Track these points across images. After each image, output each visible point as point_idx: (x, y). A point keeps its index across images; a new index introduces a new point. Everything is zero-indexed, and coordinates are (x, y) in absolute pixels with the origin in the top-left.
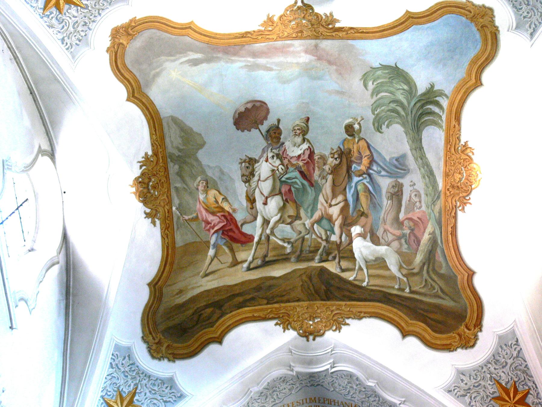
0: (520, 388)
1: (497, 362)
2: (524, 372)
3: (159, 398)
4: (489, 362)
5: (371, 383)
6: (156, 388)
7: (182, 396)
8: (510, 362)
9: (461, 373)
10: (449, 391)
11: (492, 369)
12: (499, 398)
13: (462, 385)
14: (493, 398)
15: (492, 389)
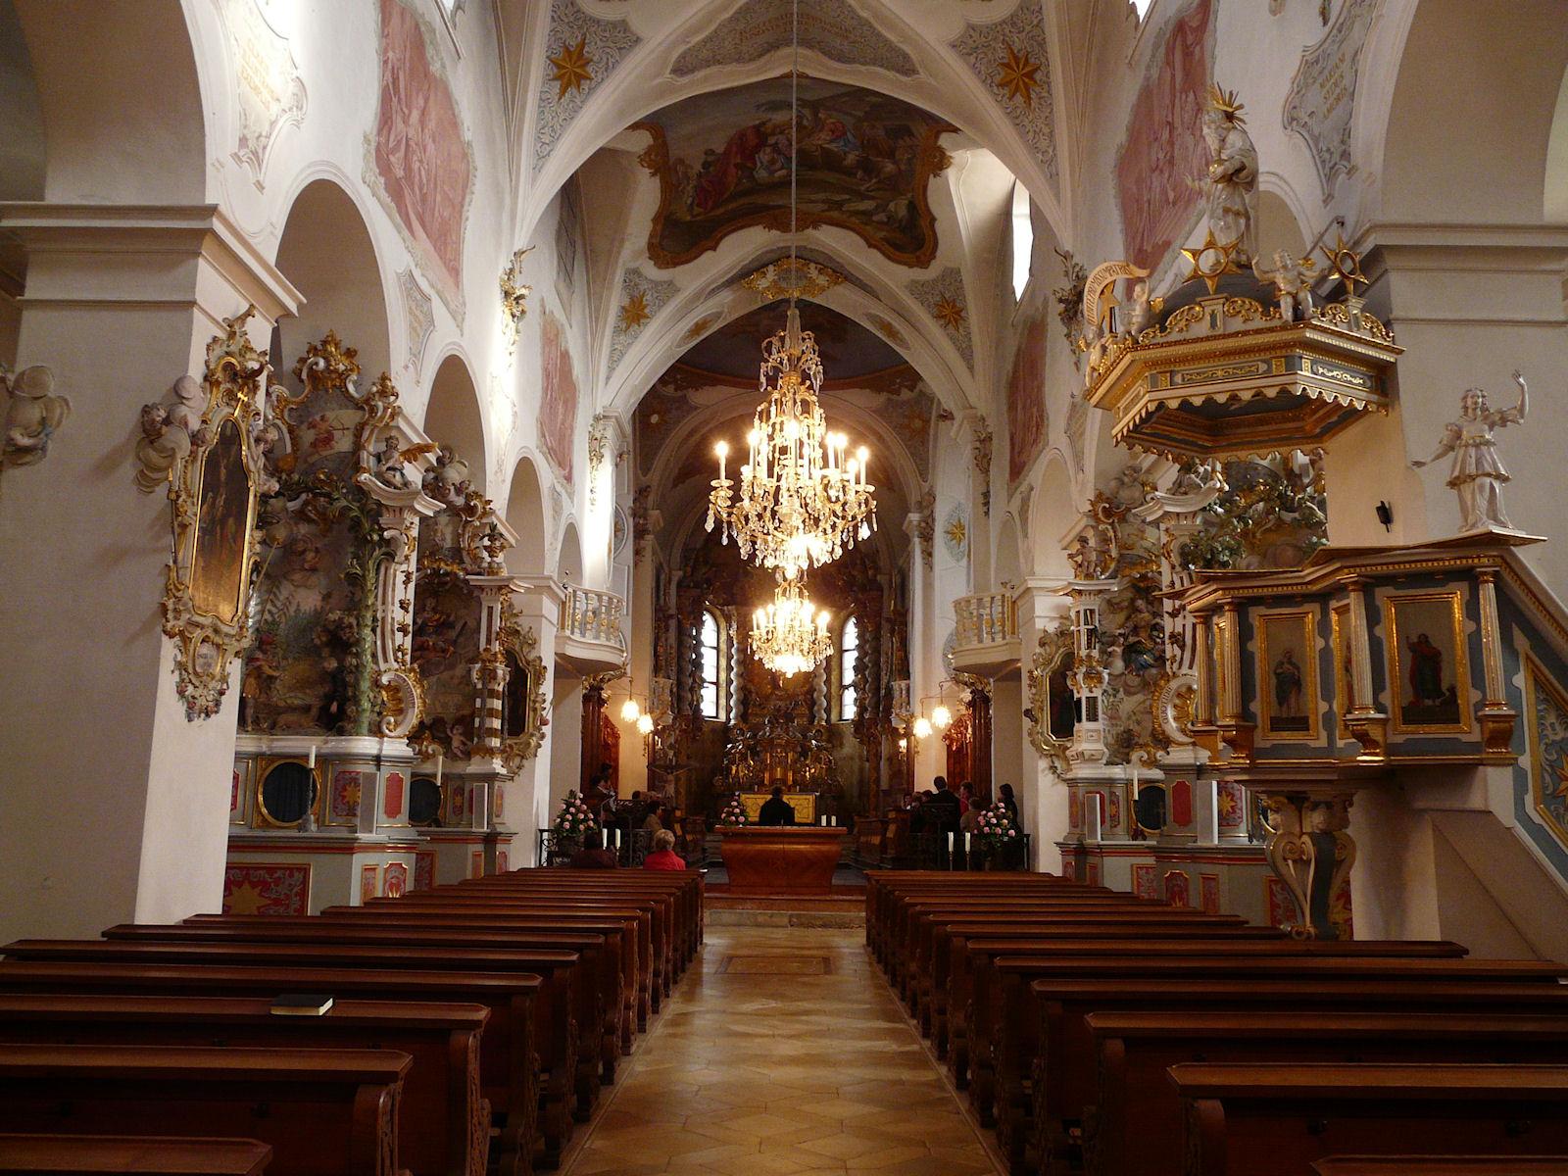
0: (1032, 61)
1: (1014, 24)
2: (1040, 45)
3: (612, 45)
4: (1004, 21)
5: (864, 14)
6: (607, 34)
7: (638, 40)
8: (1028, 28)
9: (972, 27)
10: (954, 46)
11: (1007, 31)
12: (1007, 66)
13: (971, 41)
14: (1002, 64)
15: (1001, 53)
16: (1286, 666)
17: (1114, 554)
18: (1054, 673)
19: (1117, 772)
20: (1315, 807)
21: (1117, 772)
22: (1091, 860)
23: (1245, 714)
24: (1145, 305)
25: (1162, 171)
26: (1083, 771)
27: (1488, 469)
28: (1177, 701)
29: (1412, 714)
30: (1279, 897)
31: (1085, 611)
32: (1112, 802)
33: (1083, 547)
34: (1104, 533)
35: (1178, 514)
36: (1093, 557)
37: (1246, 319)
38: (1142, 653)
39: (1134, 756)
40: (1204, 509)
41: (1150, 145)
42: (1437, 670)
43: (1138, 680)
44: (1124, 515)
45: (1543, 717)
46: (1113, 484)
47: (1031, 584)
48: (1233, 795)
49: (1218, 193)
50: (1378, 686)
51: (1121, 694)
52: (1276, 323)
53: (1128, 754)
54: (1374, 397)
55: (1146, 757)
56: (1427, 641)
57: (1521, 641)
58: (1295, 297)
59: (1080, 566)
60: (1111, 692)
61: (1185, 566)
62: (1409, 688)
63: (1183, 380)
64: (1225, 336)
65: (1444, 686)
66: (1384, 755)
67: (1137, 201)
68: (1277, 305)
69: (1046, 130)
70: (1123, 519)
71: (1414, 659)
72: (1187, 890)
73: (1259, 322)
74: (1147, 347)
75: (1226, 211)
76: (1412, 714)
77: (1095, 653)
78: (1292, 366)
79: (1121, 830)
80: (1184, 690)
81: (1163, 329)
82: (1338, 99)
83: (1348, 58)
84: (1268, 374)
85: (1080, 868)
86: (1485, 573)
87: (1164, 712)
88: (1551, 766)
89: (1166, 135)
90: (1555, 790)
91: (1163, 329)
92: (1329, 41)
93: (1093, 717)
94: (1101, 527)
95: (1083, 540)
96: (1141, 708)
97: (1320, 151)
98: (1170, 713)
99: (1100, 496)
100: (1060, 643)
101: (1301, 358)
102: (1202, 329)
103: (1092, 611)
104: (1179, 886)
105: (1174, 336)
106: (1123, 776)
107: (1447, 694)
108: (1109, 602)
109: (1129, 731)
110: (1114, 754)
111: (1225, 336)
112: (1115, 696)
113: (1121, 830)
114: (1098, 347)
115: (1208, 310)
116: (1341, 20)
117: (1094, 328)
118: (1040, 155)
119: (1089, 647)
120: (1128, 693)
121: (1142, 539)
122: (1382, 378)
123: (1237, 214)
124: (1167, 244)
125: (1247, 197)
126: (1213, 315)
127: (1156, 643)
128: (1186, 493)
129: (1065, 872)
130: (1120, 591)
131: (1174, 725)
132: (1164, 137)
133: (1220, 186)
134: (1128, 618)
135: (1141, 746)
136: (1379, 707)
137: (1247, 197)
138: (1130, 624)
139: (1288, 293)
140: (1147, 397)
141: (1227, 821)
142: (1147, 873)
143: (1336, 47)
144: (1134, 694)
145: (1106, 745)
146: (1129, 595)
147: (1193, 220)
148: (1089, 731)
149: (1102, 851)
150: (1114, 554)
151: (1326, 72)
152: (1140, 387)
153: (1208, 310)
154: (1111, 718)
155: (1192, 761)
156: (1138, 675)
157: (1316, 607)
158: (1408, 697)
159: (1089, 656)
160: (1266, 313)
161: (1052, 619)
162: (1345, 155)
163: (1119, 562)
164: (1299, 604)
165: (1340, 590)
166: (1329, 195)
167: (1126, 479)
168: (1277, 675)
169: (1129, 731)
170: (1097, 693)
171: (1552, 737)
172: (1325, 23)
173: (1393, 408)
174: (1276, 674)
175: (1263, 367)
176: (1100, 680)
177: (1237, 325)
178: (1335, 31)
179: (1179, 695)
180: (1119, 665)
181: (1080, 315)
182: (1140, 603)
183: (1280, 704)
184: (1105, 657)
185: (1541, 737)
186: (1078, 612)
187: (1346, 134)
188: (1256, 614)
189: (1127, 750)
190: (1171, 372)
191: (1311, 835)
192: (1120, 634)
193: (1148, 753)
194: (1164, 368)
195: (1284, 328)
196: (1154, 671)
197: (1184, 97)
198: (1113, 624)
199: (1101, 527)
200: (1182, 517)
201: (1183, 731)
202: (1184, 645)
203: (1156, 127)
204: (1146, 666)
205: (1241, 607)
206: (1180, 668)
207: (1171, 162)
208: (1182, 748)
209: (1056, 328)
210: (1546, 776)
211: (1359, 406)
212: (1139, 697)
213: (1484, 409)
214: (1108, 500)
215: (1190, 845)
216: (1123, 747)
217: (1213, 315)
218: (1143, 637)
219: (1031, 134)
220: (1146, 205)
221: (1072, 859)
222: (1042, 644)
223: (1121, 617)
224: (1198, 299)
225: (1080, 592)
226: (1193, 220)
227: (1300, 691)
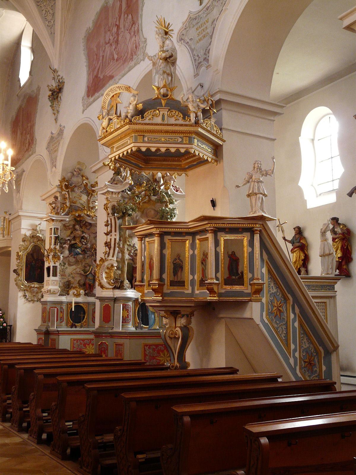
16: (178, 260)
17: (68, 204)
18: (28, 254)
19: (64, 299)
20: (183, 316)
21: (64, 299)
22: (52, 337)
23: (161, 279)
24: (134, 105)
25: (111, 45)
26: (48, 298)
27: (262, 192)
28: (107, 271)
29: (228, 282)
30: (148, 351)
31: (55, 228)
32: (61, 312)
33: (56, 200)
34: (64, 195)
35: (112, 192)
37: (176, 119)
38: (77, 248)
39: (71, 292)
40: (123, 191)
41: (105, 32)
42: (237, 265)
43: (74, 259)
44: (73, 188)
45: (269, 284)
46: (69, 175)
47: (20, 214)
48: (128, 310)
49: (160, 64)
50: (217, 271)
51: (67, 265)
52: (187, 123)
53: (68, 291)
54: (214, 157)
55: (76, 292)
56: (235, 254)
57: (265, 257)
58: (196, 114)
59: (54, 208)
60: (62, 264)
61: (113, 214)
62: (227, 272)
63: (148, 139)
64: (164, 125)
65: (239, 272)
66: (218, 297)
67: (97, 55)
68: (189, 116)
69: (51, 12)
70: (73, 190)
71: (230, 260)
72: (107, 350)
73: (181, 122)
74: (134, 124)
75: (164, 72)
76: (228, 282)
77: (58, 247)
78: (191, 142)
79: (64, 324)
80: (110, 266)
81: (143, 117)
82: (204, 37)
83: (210, 22)
84: (181, 143)
85: (46, 340)
86: (257, 230)
87: (102, 275)
88: (271, 302)
89: (115, 29)
90: (271, 311)
91: (143, 117)
92: (202, 12)
93: (55, 275)
94: (63, 193)
95: (56, 198)
96: (74, 272)
97: (194, 55)
98: (104, 275)
99: (63, 179)
100: (31, 241)
101: (194, 138)
102: (159, 120)
103: (57, 229)
104: (104, 348)
105: (147, 121)
106: (66, 301)
107: (240, 274)
108: (64, 225)
109: (69, 282)
110: (63, 290)
111: (164, 125)
112: (64, 266)
113: (64, 324)
114: (107, 119)
115: (161, 113)
116: (208, 5)
117: (106, 111)
118: (47, 22)
119: (55, 244)
120: (70, 265)
121: (80, 199)
122: (217, 149)
123: (168, 74)
124: (111, 77)
125: (172, 68)
126: (163, 116)
127: (83, 244)
128: (116, 184)
129: (38, 342)
130: (69, 221)
131: (105, 280)
132: (113, 31)
133: (161, 61)
134: (72, 233)
135: (74, 288)
136: (217, 279)
137: (172, 68)
138: (72, 235)
139: (194, 112)
140: (132, 145)
141: (125, 321)
142: (77, 342)
143: (205, 16)
144: (73, 265)
145: (60, 287)
146: (72, 223)
147: (127, 69)
148: (53, 281)
149: (58, 333)
150: (68, 204)
151: (200, 24)
152: (127, 140)
153: (161, 113)
154: (62, 275)
155: (112, 296)
156: (74, 258)
157: (190, 238)
158: (227, 275)
159: (55, 248)
160: (184, 118)
161: (29, 230)
162: (206, 60)
163: (69, 208)
164: (184, 236)
165: (204, 231)
166: (197, 74)
167: (75, 173)
168: (174, 264)
169: (69, 282)
170: (57, 264)
171: (272, 291)
172: (201, 4)
173: (220, 162)
174: (173, 263)
175: (180, 140)
176: (59, 258)
177: (172, 121)
178: (205, 9)
179: (108, 268)
180: (67, 252)
181: (59, 98)
182: (77, 227)
183: (174, 275)
184: (61, 249)
185: (269, 291)
186: (52, 228)
187: (207, 51)
188: (167, 238)
189: (68, 289)
190: (143, 136)
191: (180, 327)
192: (68, 240)
193: (77, 291)
194: (141, 133)
195: (191, 126)
196: (81, 256)
197: (126, 16)
198: (65, 235)
199: (63, 193)
200: (114, 194)
201: (109, 283)
202: (111, 247)
203: (110, 25)
204: (78, 254)
205: (162, 235)
206: (108, 256)
207: (117, 42)
208: (108, 290)
209: (44, 101)
210: (270, 305)
211: (209, 160)
212: (74, 267)
213: (260, 169)
214: (67, 181)
215: (110, 331)
216: (66, 288)
217: (163, 116)
218: (77, 241)
219: (44, 12)
220: (101, 58)
221: (43, 337)
222: (24, 241)
223: (69, 232)
224: (158, 108)
225: (53, 220)
226: (127, 69)
227: (182, 270)
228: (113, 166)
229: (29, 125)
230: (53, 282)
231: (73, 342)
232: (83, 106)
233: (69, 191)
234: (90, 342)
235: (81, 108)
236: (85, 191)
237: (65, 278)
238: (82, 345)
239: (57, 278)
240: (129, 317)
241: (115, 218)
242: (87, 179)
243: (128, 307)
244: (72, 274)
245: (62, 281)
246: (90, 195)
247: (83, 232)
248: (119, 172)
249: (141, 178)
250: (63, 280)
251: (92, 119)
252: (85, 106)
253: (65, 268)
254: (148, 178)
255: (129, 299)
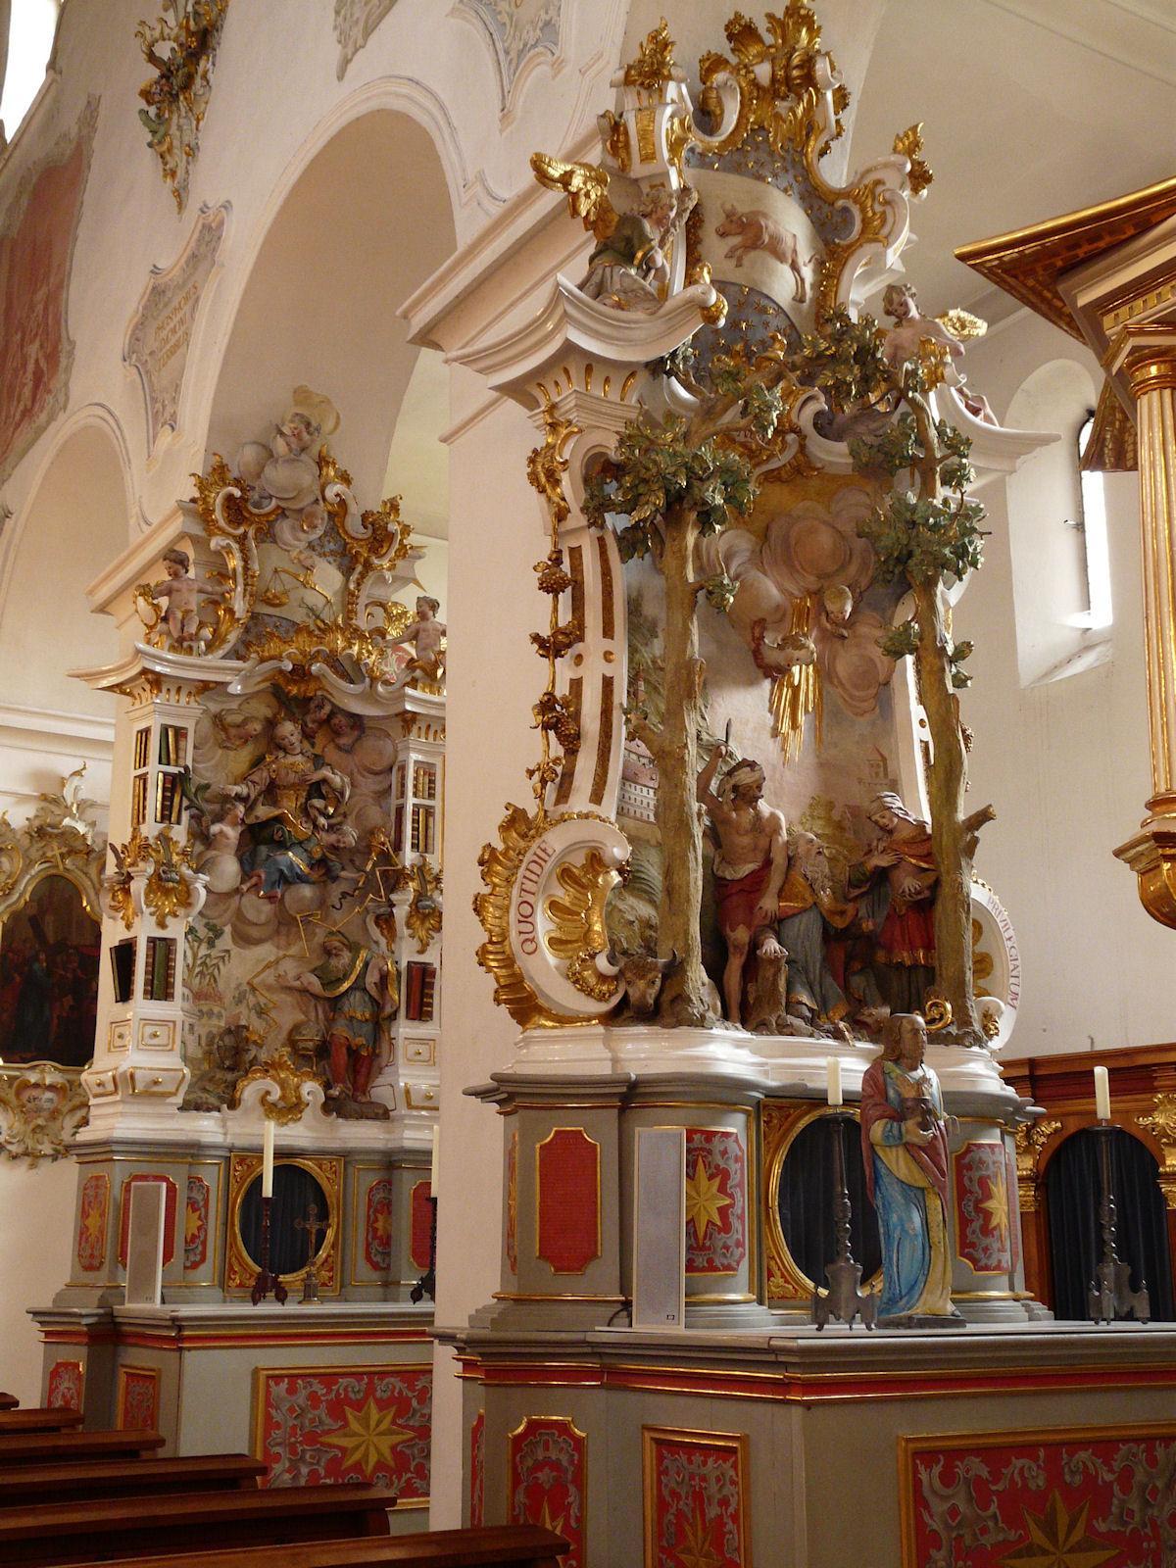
17: (240, 606)
18: (15, 917)
19: (207, 1128)
21: (207, 1128)
22: (138, 1358)
26: (116, 1122)
28: (563, 894)
30: (939, 1507)
31: (165, 729)
32: (193, 1205)
33: (175, 575)
34: (220, 555)
36: (194, 601)
38: (283, 845)
39: (251, 1090)
43: (267, 908)
44: (271, 524)
46: (250, 454)
48: (725, 1175)
51: (226, 941)
53: (233, 1086)
55: (276, 1093)
59: (165, 619)
60: (203, 932)
61: (596, 510)
70: (267, 535)
72: (580, 1480)
77: (180, 833)
79: (205, 1275)
80: (578, 860)
85: (99, 1380)
87: (526, 919)
93: (159, 989)
94: (215, 543)
95: (176, 560)
96: (269, 977)
98: (544, 925)
99: (220, 472)
100: (34, 854)
103: (181, 733)
104: (555, 1466)
106: (219, 1139)
108: (218, 721)
109: (236, 1031)
110: (201, 1081)
112: (211, 944)
113: (205, 1275)
119: (166, 816)
120: (243, 939)
121: (304, 585)
127: (316, 826)
129: (51, 1391)
130: (247, 698)
131: (551, 959)
134: (257, 762)
135: (268, 1068)
138: (262, 776)
141: (704, 1254)
142: (292, 1390)
144: (258, 942)
145: (185, 1058)
146: (263, 709)
148: (147, 1021)
149: (178, 1335)
150: (240, 606)
154: (198, 996)
155: (604, 1070)
156: (270, 898)
159: (164, 839)
161: (23, 799)
163: (247, 630)
167: (280, 447)
169: (236, 1031)
170: (176, 929)
176: (186, 901)
179: (566, 875)
180: (229, 868)
181: (198, 81)
182: (288, 729)
184: (199, 847)
186: (146, 732)
189: (230, 1077)
192: (239, 798)
193: (283, 1084)
196: (307, 891)
198: (222, 770)
199: (215, 543)
200: (598, 375)
201: (577, 980)
202: (578, 736)
204: (288, 879)
206: (563, 796)
208: (568, 1030)
212: (266, 951)
215: (604, 1333)
216: (223, 1067)
218: (289, 806)
221: (78, 1355)
223: (242, 758)
225: (156, 681)
228: (593, 197)
229: (41, 294)
230: (149, 1030)
231: (268, 1392)
232: (343, 39)
233: (245, 535)
234: (370, 1390)
235: (334, 52)
236: (332, 546)
237: (216, 1010)
238: (322, 1412)
239: (170, 1011)
240: (736, 1224)
241: (601, 541)
242: (345, 479)
243: (724, 1153)
244: (254, 989)
245: (203, 1031)
246: (359, 568)
247: (318, 761)
248: (629, 241)
249: (755, 319)
250: (204, 1020)
251: (403, 74)
252: (357, 32)
253: (214, 953)
254: (792, 325)
255: (723, 1092)
